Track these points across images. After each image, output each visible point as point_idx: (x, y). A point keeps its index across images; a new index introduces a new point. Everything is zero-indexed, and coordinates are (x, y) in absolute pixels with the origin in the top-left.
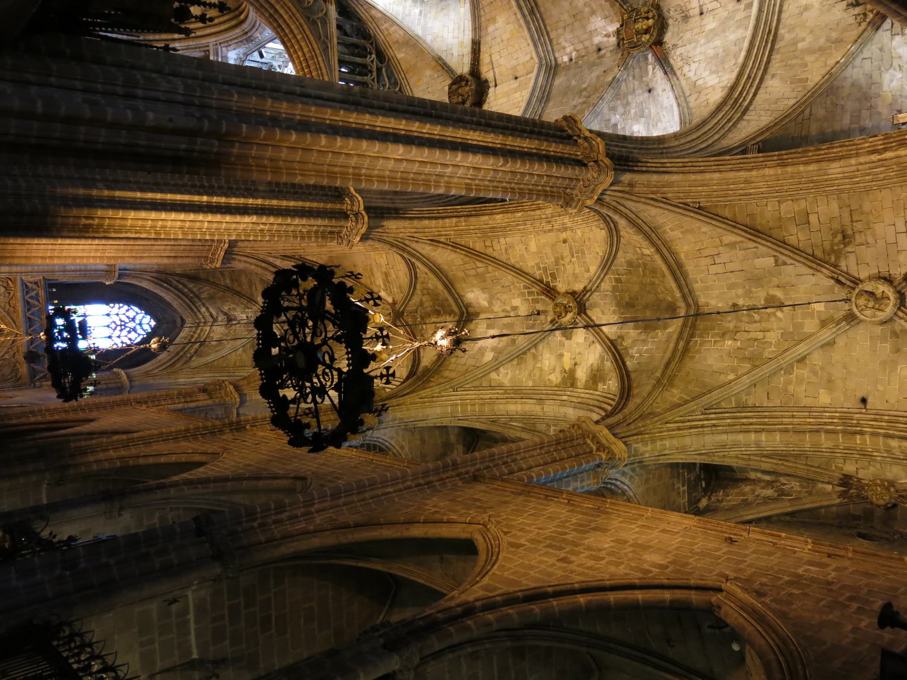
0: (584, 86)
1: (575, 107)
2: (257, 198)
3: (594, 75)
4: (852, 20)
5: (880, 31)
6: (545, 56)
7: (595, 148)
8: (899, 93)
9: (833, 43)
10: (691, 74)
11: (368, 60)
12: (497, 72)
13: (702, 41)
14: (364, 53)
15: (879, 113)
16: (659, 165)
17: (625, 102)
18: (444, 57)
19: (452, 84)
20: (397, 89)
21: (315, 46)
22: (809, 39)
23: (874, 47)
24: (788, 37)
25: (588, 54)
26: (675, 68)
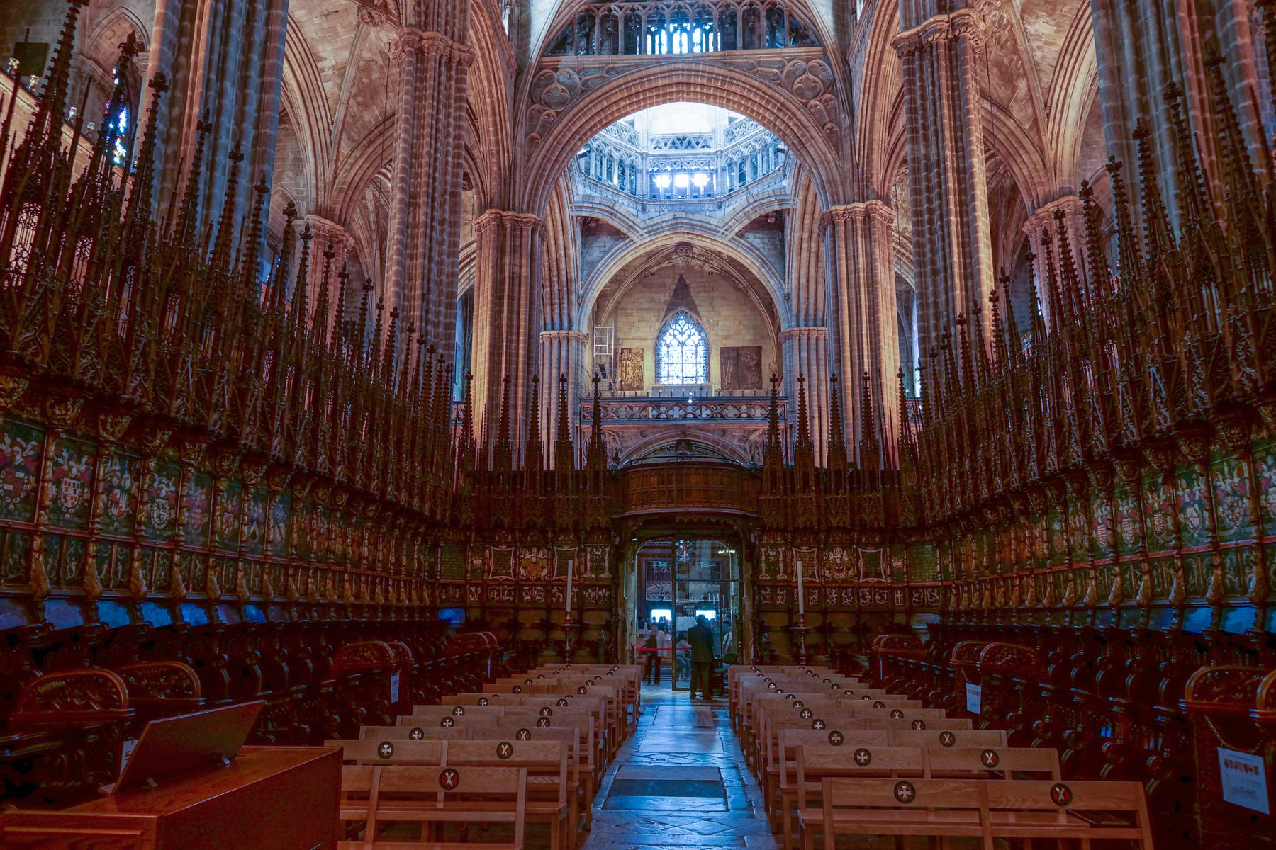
2: (945, 157)
11: (619, 13)
14: (609, 18)
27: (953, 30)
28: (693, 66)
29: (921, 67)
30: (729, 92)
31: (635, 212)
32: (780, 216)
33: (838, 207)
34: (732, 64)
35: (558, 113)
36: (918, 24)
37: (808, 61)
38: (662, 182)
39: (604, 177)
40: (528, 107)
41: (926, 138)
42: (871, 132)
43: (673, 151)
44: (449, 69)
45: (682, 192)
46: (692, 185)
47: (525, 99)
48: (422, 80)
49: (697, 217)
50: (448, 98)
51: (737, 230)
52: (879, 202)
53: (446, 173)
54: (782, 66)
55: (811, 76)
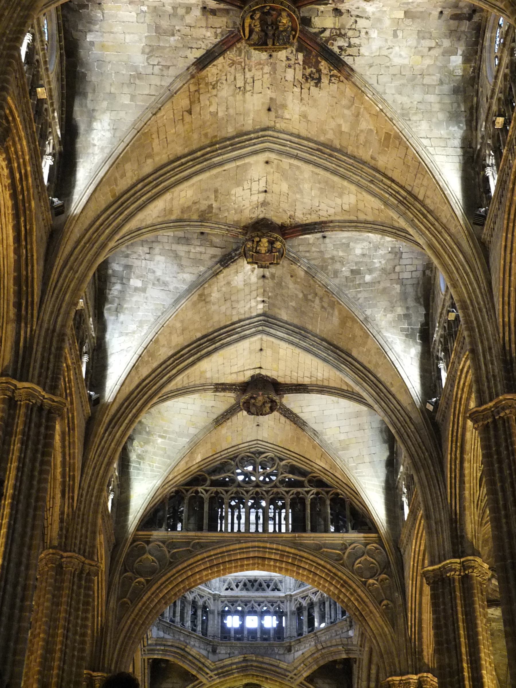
0: (301, 295)
1: (323, 307)
2: (463, 668)
3: (291, 286)
4: (334, 87)
5: (354, 67)
6: (255, 327)
7: (509, 402)
8: (413, 50)
9: (353, 104)
10: (331, 211)
12: (249, 367)
13: (298, 196)
14: (197, 499)
15: (429, 66)
16: (507, 328)
17: (330, 261)
18: (215, 417)
19: (249, 412)
20: (233, 463)
21: (199, 557)
22: (341, 122)
23: (368, 73)
24: (330, 135)
25: (264, 287)
26: (318, 220)
27: (465, 570)
28: (268, 545)
29: (443, 593)
30: (299, 567)
31: (204, 653)
32: (348, 663)
33: (395, 678)
34: (301, 544)
35: (148, 581)
36: (440, 562)
37: (366, 545)
38: (232, 622)
39: (178, 619)
40: (121, 575)
41: (448, 650)
42: (420, 613)
43: (244, 593)
44: (80, 579)
45: (252, 632)
46: (261, 626)
47: (120, 568)
48: (60, 589)
49: (266, 660)
50: (78, 602)
51: (305, 675)
52: (430, 675)
53: (71, 664)
54: (344, 547)
55: (369, 558)
